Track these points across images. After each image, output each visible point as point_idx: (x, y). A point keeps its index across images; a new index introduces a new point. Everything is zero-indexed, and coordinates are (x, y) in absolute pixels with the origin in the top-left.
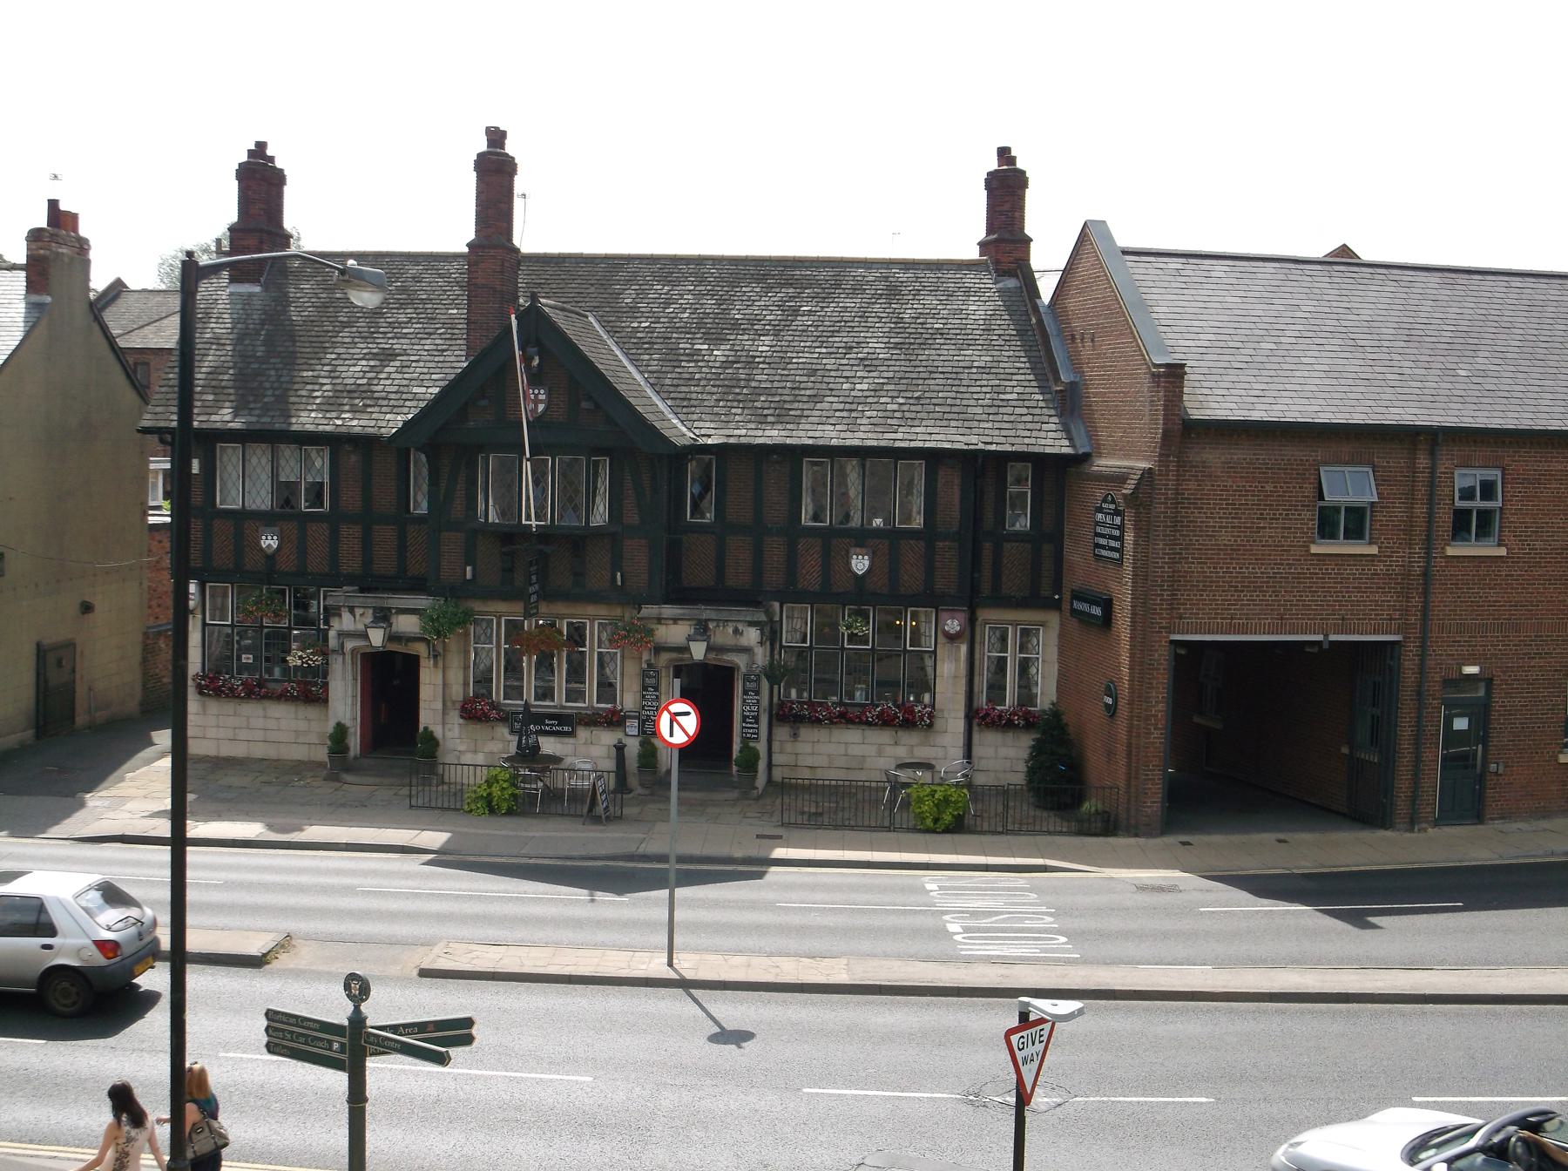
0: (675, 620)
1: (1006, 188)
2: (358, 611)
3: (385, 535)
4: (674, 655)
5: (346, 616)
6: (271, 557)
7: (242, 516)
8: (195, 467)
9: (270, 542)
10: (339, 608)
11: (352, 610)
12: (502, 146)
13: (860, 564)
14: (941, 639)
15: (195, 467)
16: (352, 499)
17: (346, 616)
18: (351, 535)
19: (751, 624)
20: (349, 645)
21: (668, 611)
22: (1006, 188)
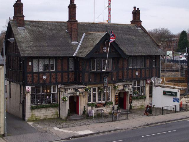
0: (120, 85)
1: (136, 13)
2: (71, 89)
3: (65, 74)
4: (120, 91)
5: (69, 90)
6: (44, 80)
7: (38, 73)
8: (30, 64)
9: (45, 77)
10: (67, 89)
11: (69, 89)
12: (74, 3)
13: (137, 73)
14: (146, 84)
15: (30, 64)
16: (59, 68)
17: (69, 90)
18: (59, 75)
19: (131, 85)
20: (69, 96)
21: (120, 84)
22: (136, 13)
